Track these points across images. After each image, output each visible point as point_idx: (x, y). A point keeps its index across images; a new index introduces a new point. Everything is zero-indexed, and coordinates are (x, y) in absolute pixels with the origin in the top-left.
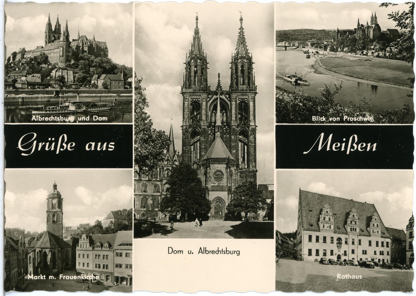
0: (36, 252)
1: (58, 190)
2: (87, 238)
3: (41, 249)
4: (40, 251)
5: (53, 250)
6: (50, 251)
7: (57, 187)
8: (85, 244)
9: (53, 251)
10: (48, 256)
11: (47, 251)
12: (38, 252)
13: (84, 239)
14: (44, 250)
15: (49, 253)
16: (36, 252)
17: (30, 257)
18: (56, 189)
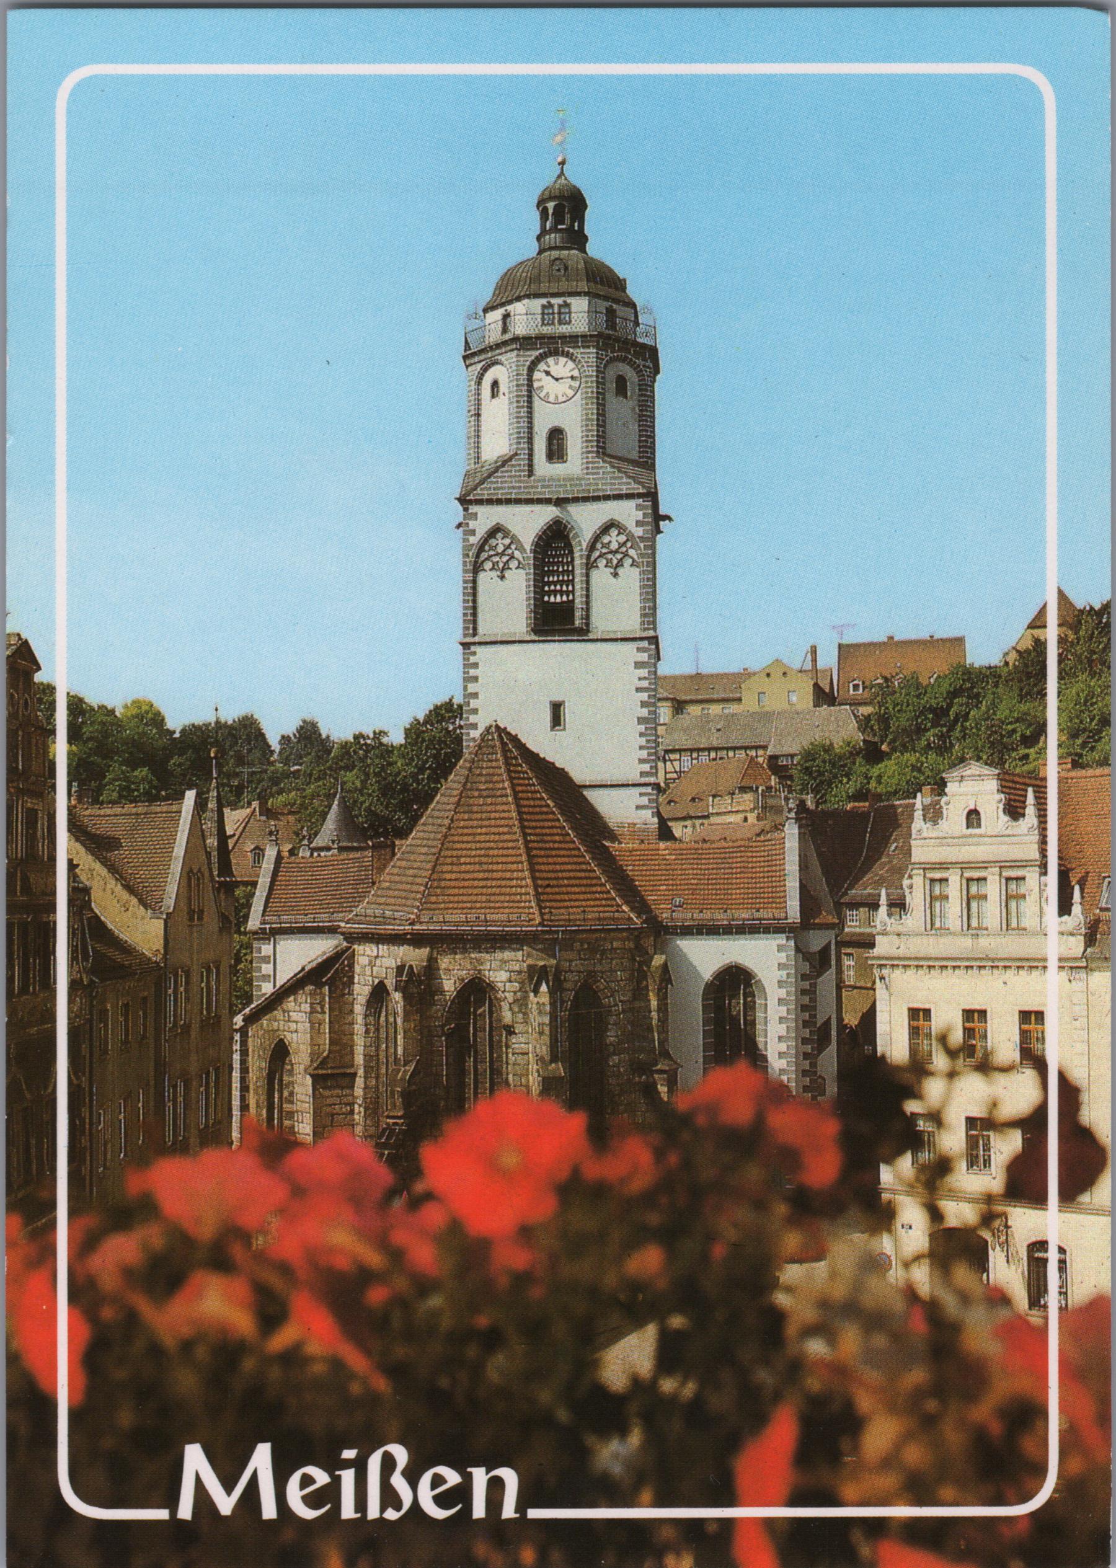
0: (361, 991)
1: (594, 249)
2: (1014, 811)
3: (415, 956)
4: (419, 986)
5: (575, 965)
6: (535, 976)
7: (590, 215)
8: (993, 888)
9: (572, 980)
10: (518, 1042)
11: (502, 970)
12: (379, 993)
13: (973, 817)
14: (452, 974)
15: (521, 1003)
16: (361, 991)
17: (280, 1053)
18: (578, 239)
